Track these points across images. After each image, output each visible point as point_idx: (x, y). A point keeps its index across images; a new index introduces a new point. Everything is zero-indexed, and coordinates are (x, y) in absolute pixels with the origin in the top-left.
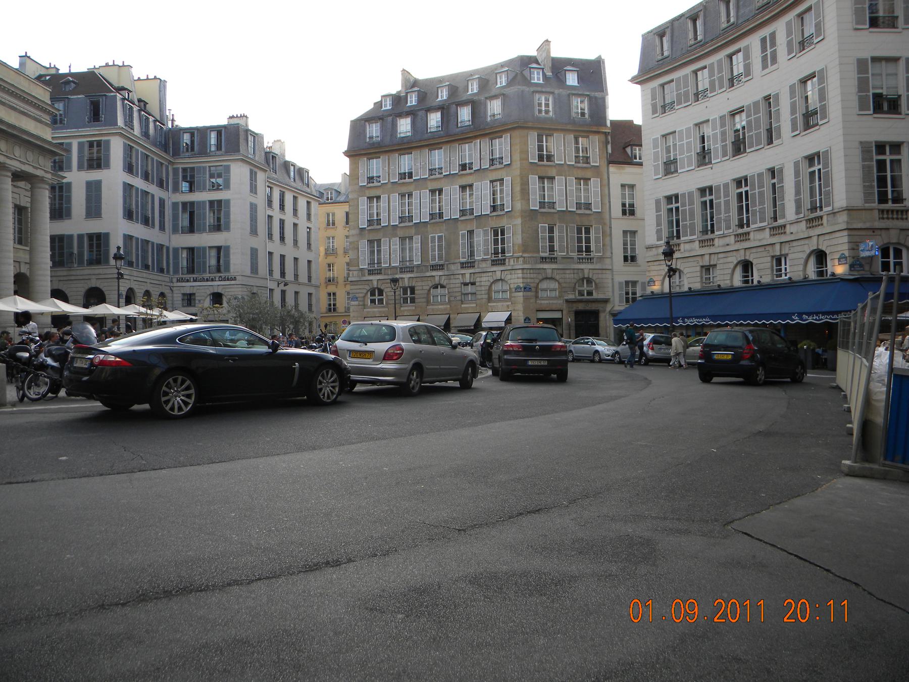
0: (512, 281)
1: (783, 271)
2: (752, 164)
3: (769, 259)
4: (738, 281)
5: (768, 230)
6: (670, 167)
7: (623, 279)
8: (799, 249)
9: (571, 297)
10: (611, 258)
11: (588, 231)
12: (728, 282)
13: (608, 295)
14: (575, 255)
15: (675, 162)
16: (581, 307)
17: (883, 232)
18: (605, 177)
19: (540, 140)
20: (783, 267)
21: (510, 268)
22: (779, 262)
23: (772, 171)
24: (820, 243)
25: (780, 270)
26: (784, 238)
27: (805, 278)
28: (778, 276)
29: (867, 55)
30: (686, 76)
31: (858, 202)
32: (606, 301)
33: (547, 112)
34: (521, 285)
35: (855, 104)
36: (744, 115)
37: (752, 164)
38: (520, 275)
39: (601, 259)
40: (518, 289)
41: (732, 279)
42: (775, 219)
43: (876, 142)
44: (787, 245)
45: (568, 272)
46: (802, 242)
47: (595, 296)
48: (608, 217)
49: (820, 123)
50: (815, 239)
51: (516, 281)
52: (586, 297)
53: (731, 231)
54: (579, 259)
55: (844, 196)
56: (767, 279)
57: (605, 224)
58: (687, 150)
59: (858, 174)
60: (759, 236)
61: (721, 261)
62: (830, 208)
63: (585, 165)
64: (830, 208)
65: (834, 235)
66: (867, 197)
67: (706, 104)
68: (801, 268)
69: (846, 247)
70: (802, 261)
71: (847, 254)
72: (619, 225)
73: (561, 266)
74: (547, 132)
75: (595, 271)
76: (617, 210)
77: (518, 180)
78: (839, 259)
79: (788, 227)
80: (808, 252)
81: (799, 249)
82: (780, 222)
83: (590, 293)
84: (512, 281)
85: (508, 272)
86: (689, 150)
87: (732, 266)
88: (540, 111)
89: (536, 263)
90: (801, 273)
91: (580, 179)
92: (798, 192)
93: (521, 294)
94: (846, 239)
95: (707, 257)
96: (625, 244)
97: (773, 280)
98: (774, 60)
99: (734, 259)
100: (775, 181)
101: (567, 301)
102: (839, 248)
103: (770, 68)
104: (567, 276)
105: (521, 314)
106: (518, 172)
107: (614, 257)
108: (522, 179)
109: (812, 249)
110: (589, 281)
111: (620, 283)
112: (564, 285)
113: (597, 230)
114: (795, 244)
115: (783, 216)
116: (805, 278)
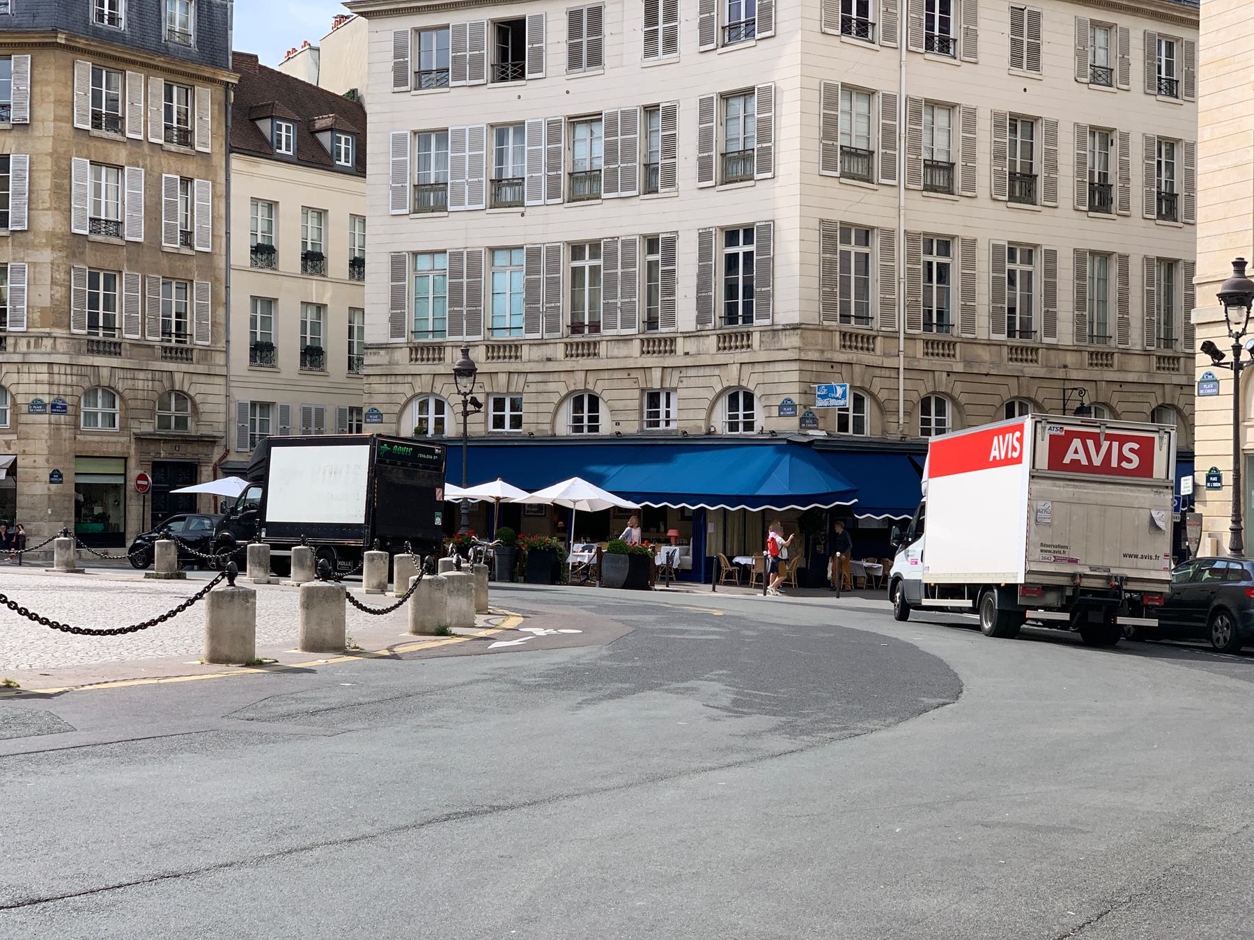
0: (22, 389)
1: (662, 416)
2: (619, 218)
3: (637, 393)
4: (564, 428)
5: (637, 343)
6: (429, 198)
7: (247, 397)
8: (701, 382)
9: (148, 427)
10: (227, 352)
11: (110, 282)
12: (547, 427)
13: (218, 430)
14: (155, 339)
15: (441, 186)
16: (164, 454)
17: (845, 369)
18: (222, 179)
19: (97, 81)
20: (662, 409)
21: (17, 358)
22: (653, 398)
23: (652, 243)
24: (745, 376)
25: (657, 414)
26: (669, 361)
27: (709, 433)
28: (650, 424)
29: (837, 78)
30: (477, 27)
31: (813, 318)
32: (211, 441)
33: (113, 19)
34: (46, 399)
35: (816, 156)
36: (600, 129)
37: (619, 218)
38: (45, 377)
39: (207, 352)
40: (36, 406)
41: (553, 423)
42: (652, 323)
43: (841, 223)
44: (676, 374)
45: (141, 375)
46: (708, 371)
47: (192, 429)
48: (223, 265)
49: (757, 176)
50: (735, 368)
51: (33, 388)
52: (173, 430)
53: (558, 335)
54: (165, 349)
55: (796, 305)
56: (632, 427)
57: (216, 280)
58: (470, 167)
59: (815, 271)
60: (621, 350)
61: (533, 388)
62: (767, 322)
63: (183, 149)
64: (767, 322)
65: (771, 367)
66: (827, 307)
67: (519, 91)
68: (703, 415)
69: (796, 388)
70: (706, 404)
71: (796, 399)
72: (246, 284)
73: (127, 364)
74: (113, 64)
75: (195, 378)
76: (241, 253)
77: (48, 163)
78: (781, 408)
79: (680, 341)
80: (719, 389)
81: (701, 382)
82: (663, 331)
83: (181, 422)
84: (22, 389)
85: (14, 368)
86: (476, 171)
87: (556, 399)
88: (101, 16)
89: (79, 353)
90: (702, 424)
91: (100, 164)
92: (703, 283)
93: (45, 418)
94: (795, 376)
95: (503, 378)
96: (253, 321)
97: (642, 430)
98: (671, 42)
99: (560, 388)
100: (657, 257)
101: (140, 439)
102: (782, 389)
103: (662, 57)
104: (140, 384)
105: (41, 461)
106: (47, 146)
107: (232, 351)
108: (56, 162)
109: (726, 385)
110: (182, 396)
111: (242, 406)
112: (132, 404)
113: (202, 290)
114: (692, 372)
115: (671, 321)
116: (709, 433)
